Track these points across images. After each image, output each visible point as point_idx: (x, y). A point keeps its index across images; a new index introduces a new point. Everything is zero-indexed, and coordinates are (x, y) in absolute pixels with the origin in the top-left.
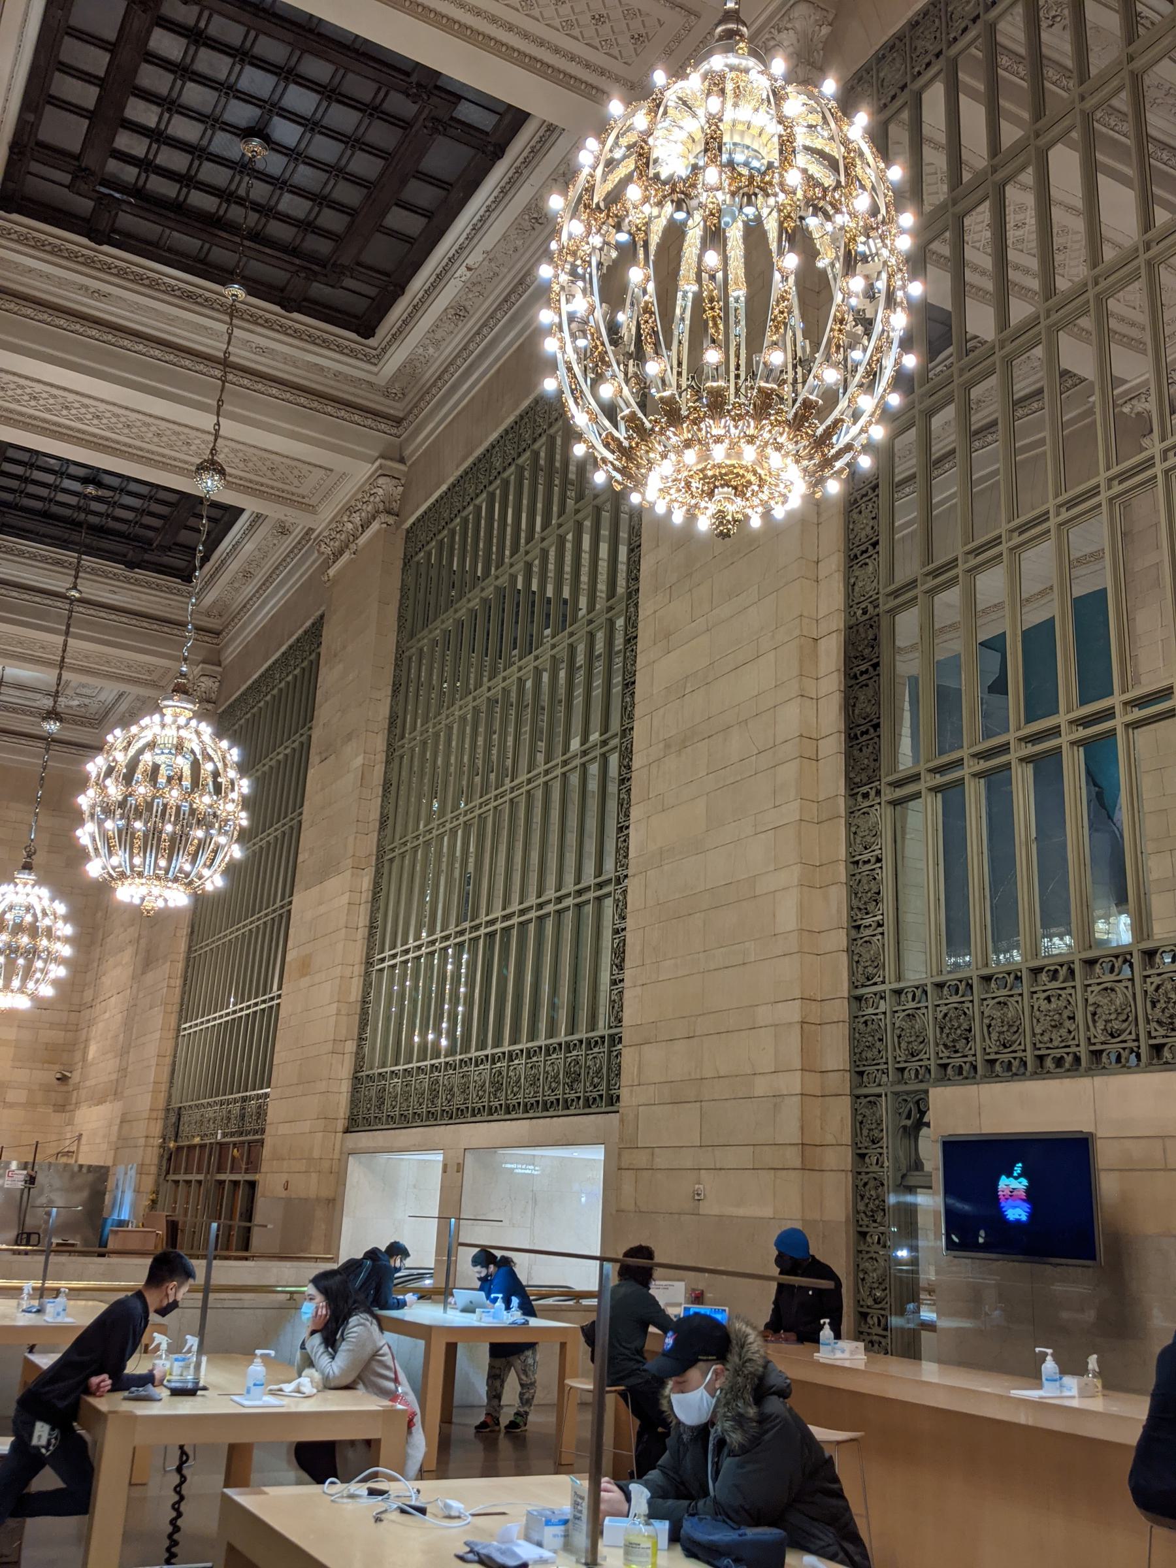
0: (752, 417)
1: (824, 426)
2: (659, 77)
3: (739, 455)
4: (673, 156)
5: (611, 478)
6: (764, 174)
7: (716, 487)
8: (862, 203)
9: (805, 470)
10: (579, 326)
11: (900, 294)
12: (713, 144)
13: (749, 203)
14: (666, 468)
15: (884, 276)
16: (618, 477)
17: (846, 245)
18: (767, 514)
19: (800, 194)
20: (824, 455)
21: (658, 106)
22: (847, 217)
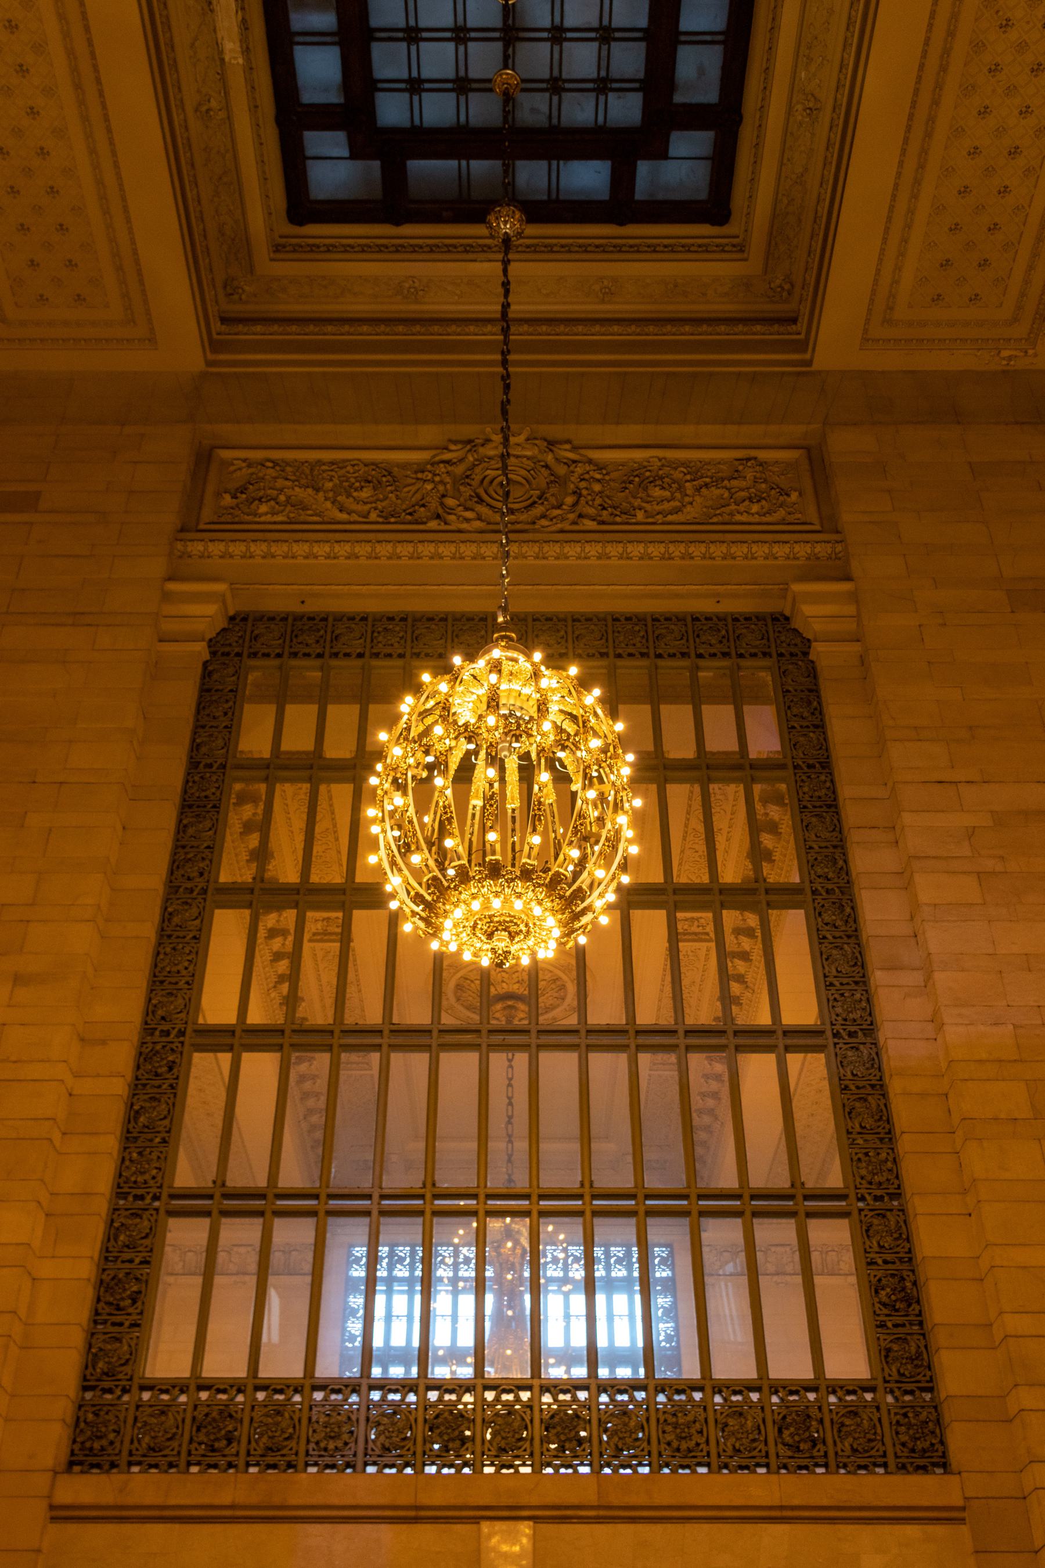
0: (520, 879)
1: (571, 890)
2: (457, 660)
3: (512, 907)
4: (465, 713)
5: (417, 928)
6: (528, 723)
7: (497, 930)
8: (595, 743)
9: (560, 921)
10: (397, 819)
11: (626, 806)
12: (493, 702)
13: (517, 741)
14: (458, 913)
15: (612, 793)
16: (422, 925)
17: (584, 770)
18: (533, 954)
19: (552, 737)
20: (573, 911)
21: (456, 678)
22: (584, 753)
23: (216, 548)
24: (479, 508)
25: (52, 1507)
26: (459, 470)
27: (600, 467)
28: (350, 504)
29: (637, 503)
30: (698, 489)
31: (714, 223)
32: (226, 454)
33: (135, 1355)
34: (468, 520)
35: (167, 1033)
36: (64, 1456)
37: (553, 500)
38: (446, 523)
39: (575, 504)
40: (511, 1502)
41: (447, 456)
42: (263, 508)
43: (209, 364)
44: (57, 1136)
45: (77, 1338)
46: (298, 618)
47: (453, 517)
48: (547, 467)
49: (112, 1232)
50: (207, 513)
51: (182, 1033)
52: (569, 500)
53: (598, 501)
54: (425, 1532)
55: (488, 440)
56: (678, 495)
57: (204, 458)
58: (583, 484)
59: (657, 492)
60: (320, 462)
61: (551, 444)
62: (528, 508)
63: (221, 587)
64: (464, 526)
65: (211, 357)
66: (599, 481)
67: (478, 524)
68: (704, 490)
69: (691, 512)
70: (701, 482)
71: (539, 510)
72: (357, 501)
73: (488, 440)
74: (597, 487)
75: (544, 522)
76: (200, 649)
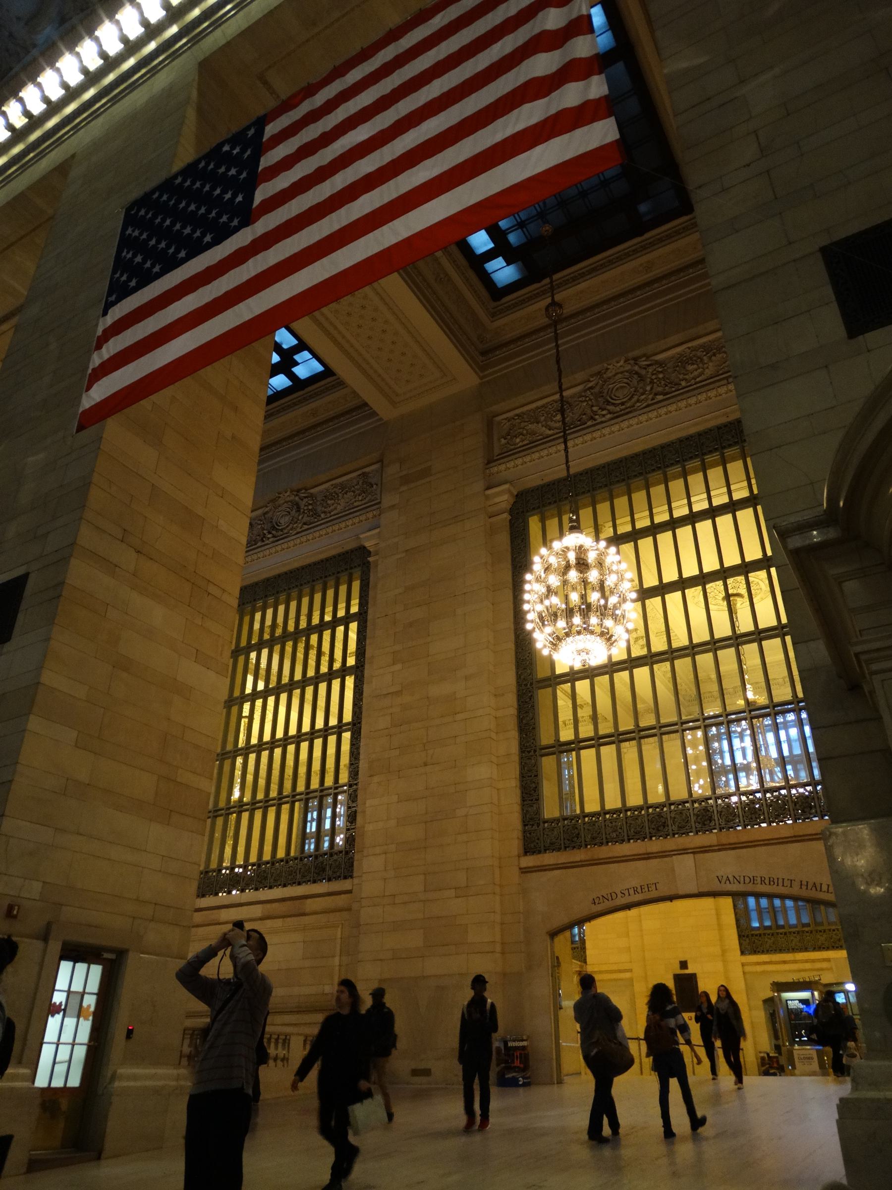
23: (503, 467)
24: (609, 407)
25: (520, 869)
26: (596, 390)
27: (660, 363)
28: (553, 424)
29: (681, 377)
30: (710, 358)
31: (686, 214)
32: (498, 419)
33: (538, 812)
34: (604, 416)
35: (526, 685)
36: (522, 851)
37: (641, 391)
38: (595, 420)
39: (652, 389)
40: (683, 847)
41: (590, 385)
42: (518, 440)
43: (481, 378)
44: (494, 735)
45: (517, 808)
46: (543, 486)
47: (597, 417)
48: (637, 373)
49: (523, 765)
50: (497, 451)
51: (531, 684)
52: (648, 388)
53: (663, 382)
54: (654, 862)
55: (607, 369)
56: (701, 365)
57: (490, 424)
58: (654, 377)
59: (690, 368)
60: (537, 408)
61: (636, 359)
62: (630, 399)
63: (506, 486)
64: (603, 419)
65: (481, 375)
66: (661, 372)
67: (609, 416)
68: (713, 358)
69: (708, 373)
70: (711, 353)
71: (636, 398)
72: (555, 422)
73: (607, 369)
74: (661, 376)
75: (638, 404)
76: (506, 516)
